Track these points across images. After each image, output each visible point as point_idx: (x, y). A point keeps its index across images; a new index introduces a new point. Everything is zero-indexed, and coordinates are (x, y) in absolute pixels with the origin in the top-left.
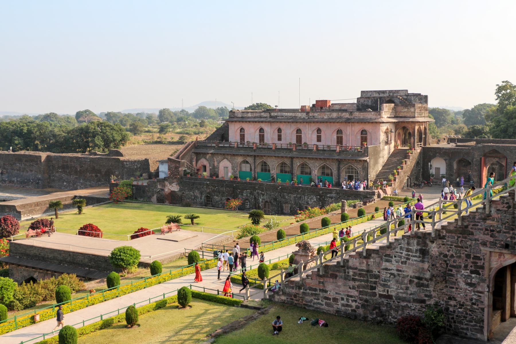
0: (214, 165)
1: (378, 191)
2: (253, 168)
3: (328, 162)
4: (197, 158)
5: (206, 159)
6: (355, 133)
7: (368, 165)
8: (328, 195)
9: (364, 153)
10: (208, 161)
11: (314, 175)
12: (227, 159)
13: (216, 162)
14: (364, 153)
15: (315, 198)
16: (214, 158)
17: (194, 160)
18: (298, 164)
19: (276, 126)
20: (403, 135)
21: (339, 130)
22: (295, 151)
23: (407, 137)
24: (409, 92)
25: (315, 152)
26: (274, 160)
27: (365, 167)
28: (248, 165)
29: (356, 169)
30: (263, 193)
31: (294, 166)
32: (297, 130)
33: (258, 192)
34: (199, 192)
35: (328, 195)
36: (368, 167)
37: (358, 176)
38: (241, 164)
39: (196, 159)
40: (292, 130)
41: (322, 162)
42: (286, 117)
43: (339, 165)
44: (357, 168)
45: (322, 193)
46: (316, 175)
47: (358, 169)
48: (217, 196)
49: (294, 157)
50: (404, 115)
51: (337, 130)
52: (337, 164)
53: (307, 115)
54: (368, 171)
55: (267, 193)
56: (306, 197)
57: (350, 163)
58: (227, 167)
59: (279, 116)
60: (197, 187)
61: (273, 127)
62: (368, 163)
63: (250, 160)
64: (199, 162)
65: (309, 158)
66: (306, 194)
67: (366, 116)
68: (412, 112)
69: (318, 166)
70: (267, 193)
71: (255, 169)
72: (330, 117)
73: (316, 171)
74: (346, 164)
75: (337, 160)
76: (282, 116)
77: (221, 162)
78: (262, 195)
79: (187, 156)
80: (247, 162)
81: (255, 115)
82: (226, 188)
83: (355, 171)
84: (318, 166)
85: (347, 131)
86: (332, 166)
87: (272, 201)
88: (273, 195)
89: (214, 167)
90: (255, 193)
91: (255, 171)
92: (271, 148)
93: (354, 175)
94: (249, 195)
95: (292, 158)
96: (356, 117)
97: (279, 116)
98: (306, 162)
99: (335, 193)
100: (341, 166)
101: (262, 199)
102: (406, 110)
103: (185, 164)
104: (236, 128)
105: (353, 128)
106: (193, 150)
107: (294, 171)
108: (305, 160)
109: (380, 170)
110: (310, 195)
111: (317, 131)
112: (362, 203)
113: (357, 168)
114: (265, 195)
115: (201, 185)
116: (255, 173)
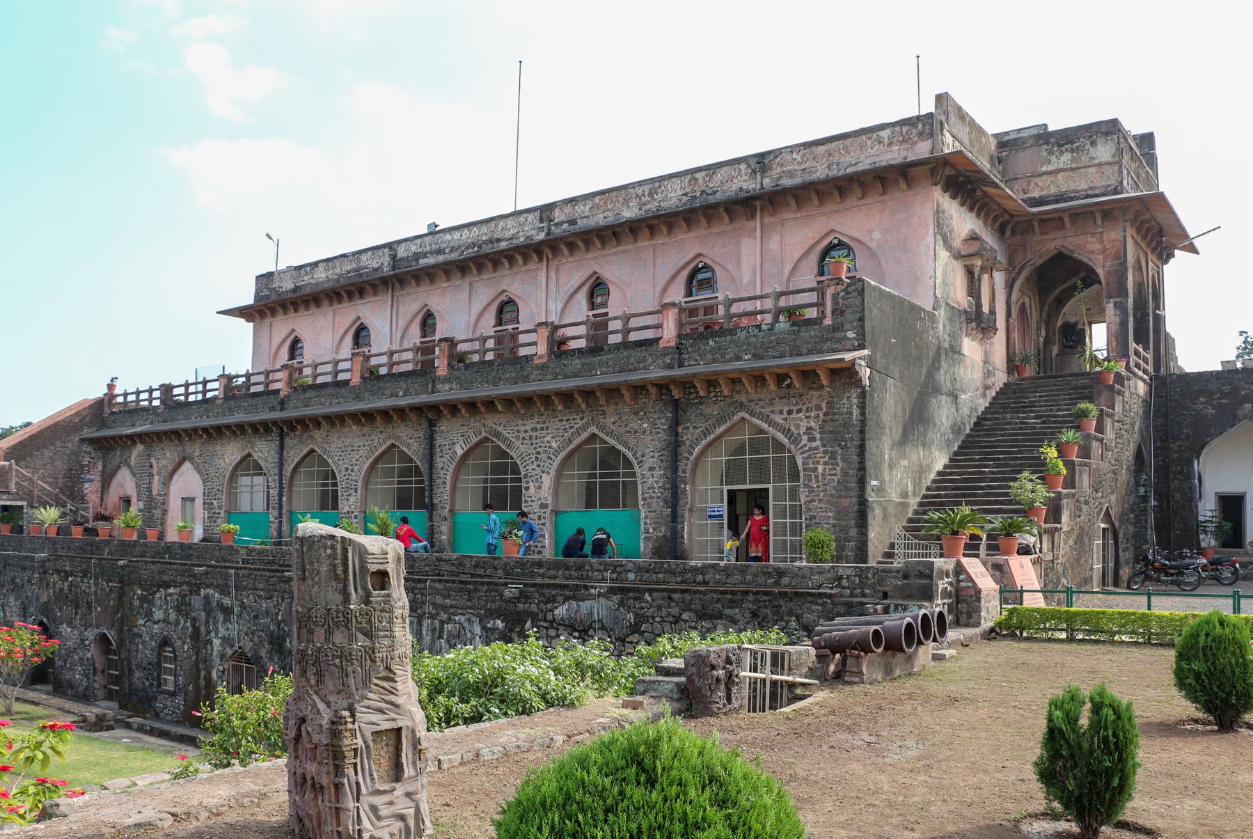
0: (151, 491)
1: (960, 569)
2: (274, 492)
3: (609, 421)
4: (104, 467)
5: (129, 466)
6: (787, 271)
7: (862, 407)
8: (561, 611)
9: (837, 328)
10: (134, 474)
11: (535, 507)
12: (192, 460)
13: (156, 478)
14: (837, 328)
15: (477, 629)
16: (153, 460)
17: (96, 475)
18: (460, 452)
19: (412, 302)
20: (1039, 329)
21: (696, 271)
22: (445, 380)
23: (1055, 350)
24: (1051, 128)
25: (543, 367)
26: (358, 442)
27: (847, 425)
28: (259, 480)
29: (779, 447)
30: (227, 601)
31: (439, 463)
32: (500, 311)
33: (207, 597)
34: (18, 603)
35: (561, 611)
36: (863, 423)
37: (794, 495)
38: (233, 477)
39: (103, 472)
40: (477, 307)
41: (580, 423)
42: (453, 250)
43: (676, 423)
44: (787, 432)
45: (523, 596)
46: (543, 506)
47: (795, 440)
48: (70, 624)
49: (435, 407)
50: (1053, 190)
51: (685, 273)
52: (663, 424)
53: (541, 220)
54: (862, 449)
55: (243, 606)
56: (426, 623)
57: (741, 406)
58: (192, 500)
59: (425, 256)
60: (13, 580)
61: (402, 310)
62: (863, 395)
63: (264, 451)
64: (114, 483)
65: (509, 402)
66: (428, 608)
67: (847, 159)
68: (1100, 165)
69: (557, 453)
70: (243, 606)
71: (281, 495)
72: (652, 206)
73: (547, 480)
74: (721, 420)
75: (663, 387)
76: (439, 252)
77: (175, 477)
78: (221, 617)
79: (47, 453)
80: (258, 470)
81: (337, 271)
82: (96, 579)
83: (779, 462)
84: (557, 453)
85: (739, 262)
86: (631, 439)
87: (263, 653)
88: (267, 613)
89: (150, 498)
90: (197, 602)
91: (281, 508)
92: (347, 382)
93: (770, 486)
94: (173, 615)
95: (430, 415)
96: (791, 174)
97: (425, 255)
98: (498, 435)
99: (612, 591)
100: (687, 436)
101: (226, 641)
102: (1067, 157)
103: (14, 480)
104: (276, 340)
105: (774, 243)
106: (87, 433)
107: (437, 491)
108: (492, 421)
109: (939, 466)
110: (451, 611)
111: (591, 296)
112: (805, 652)
113: (787, 432)
114: (234, 618)
115: (24, 568)
116: (281, 515)
